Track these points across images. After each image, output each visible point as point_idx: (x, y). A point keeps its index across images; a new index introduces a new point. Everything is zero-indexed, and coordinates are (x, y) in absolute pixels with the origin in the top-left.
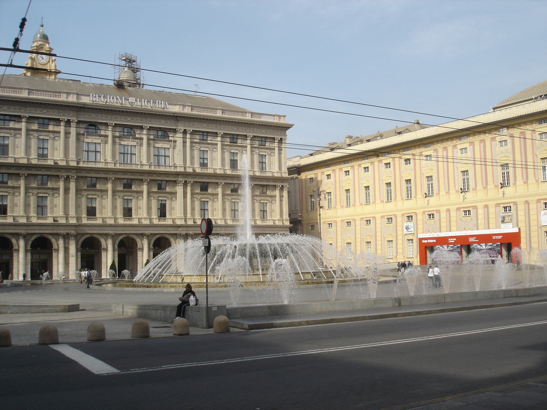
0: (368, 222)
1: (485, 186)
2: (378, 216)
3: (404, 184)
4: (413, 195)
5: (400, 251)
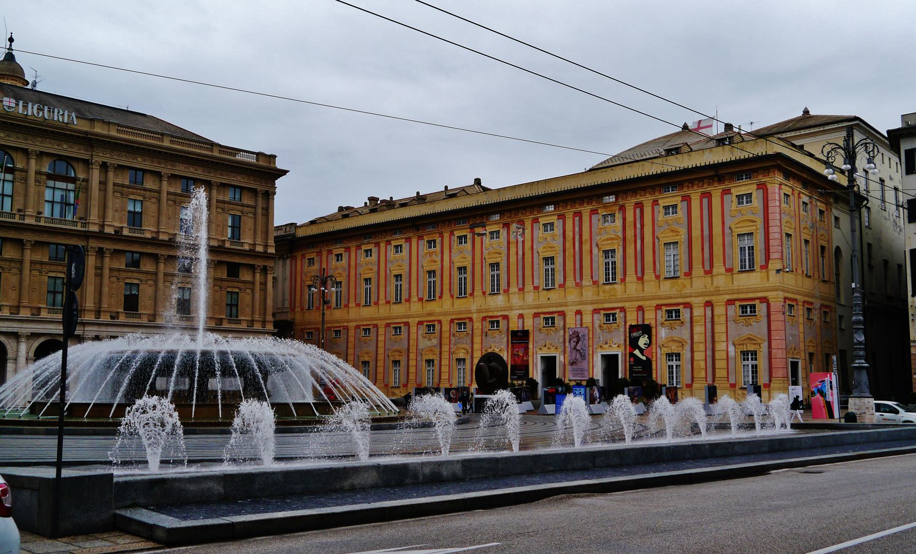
0: (397, 329)
1: (578, 281)
2: (413, 322)
3: (456, 275)
4: (469, 291)
5: (445, 376)
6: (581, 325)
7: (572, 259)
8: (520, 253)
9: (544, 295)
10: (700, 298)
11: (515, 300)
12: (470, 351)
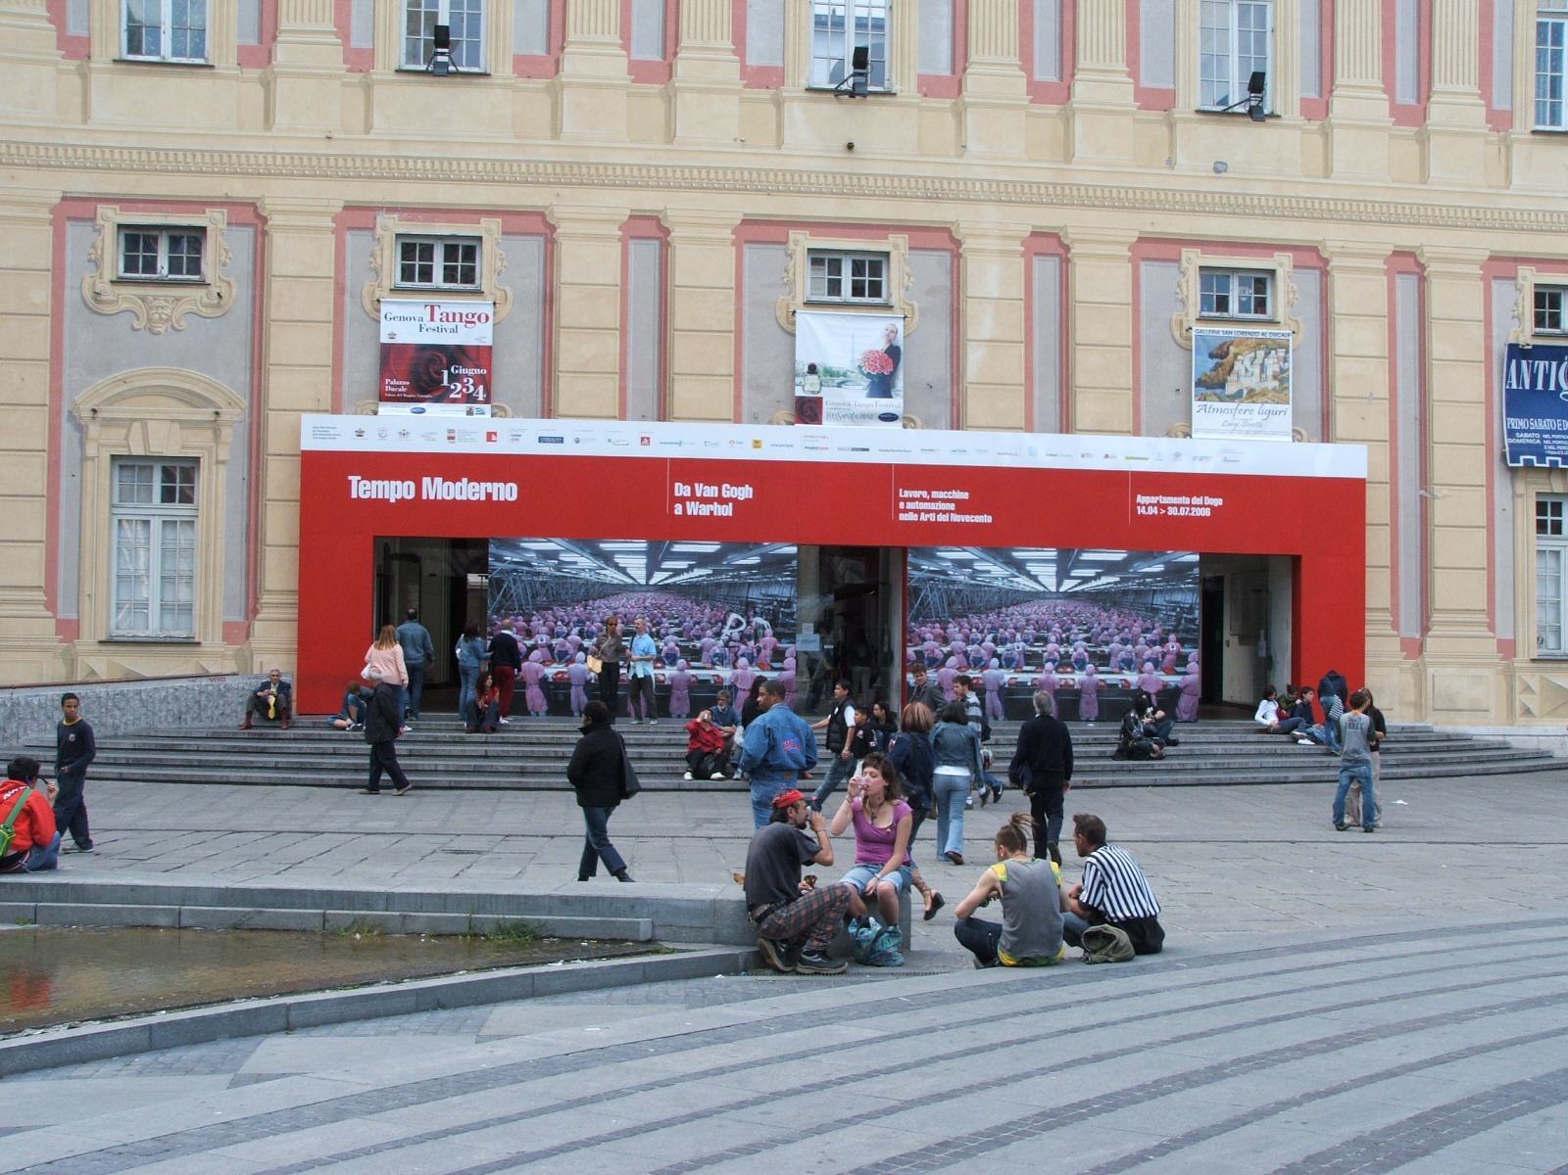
1: (1046, 73)
9: (811, 132)
12: (235, 415)
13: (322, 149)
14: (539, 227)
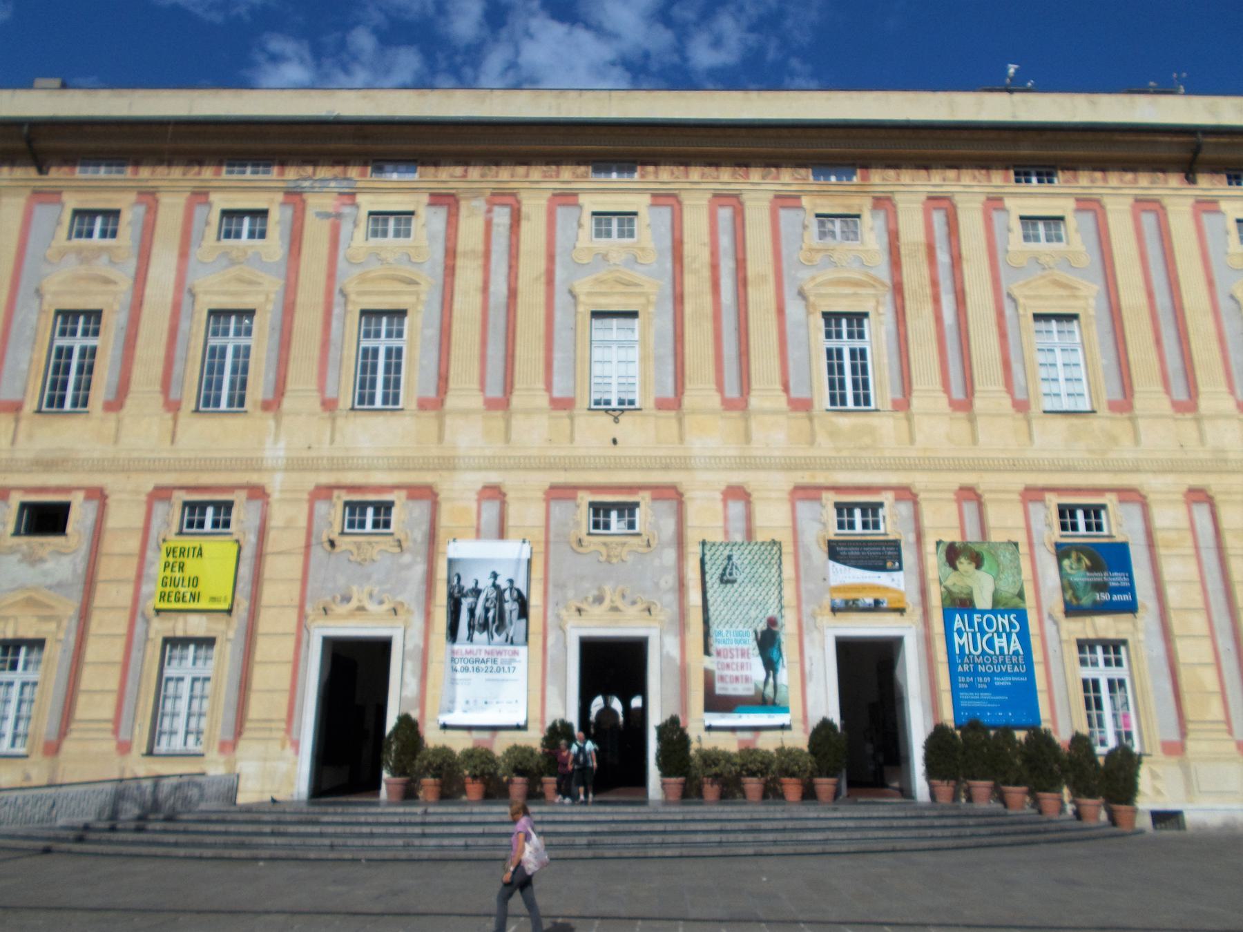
1: (732, 392)
4: (258, 389)
5: (95, 706)
6: (749, 533)
7: (708, 326)
8: (499, 287)
10: (1170, 479)
11: (469, 434)
13: (305, 454)
14: (425, 494)
